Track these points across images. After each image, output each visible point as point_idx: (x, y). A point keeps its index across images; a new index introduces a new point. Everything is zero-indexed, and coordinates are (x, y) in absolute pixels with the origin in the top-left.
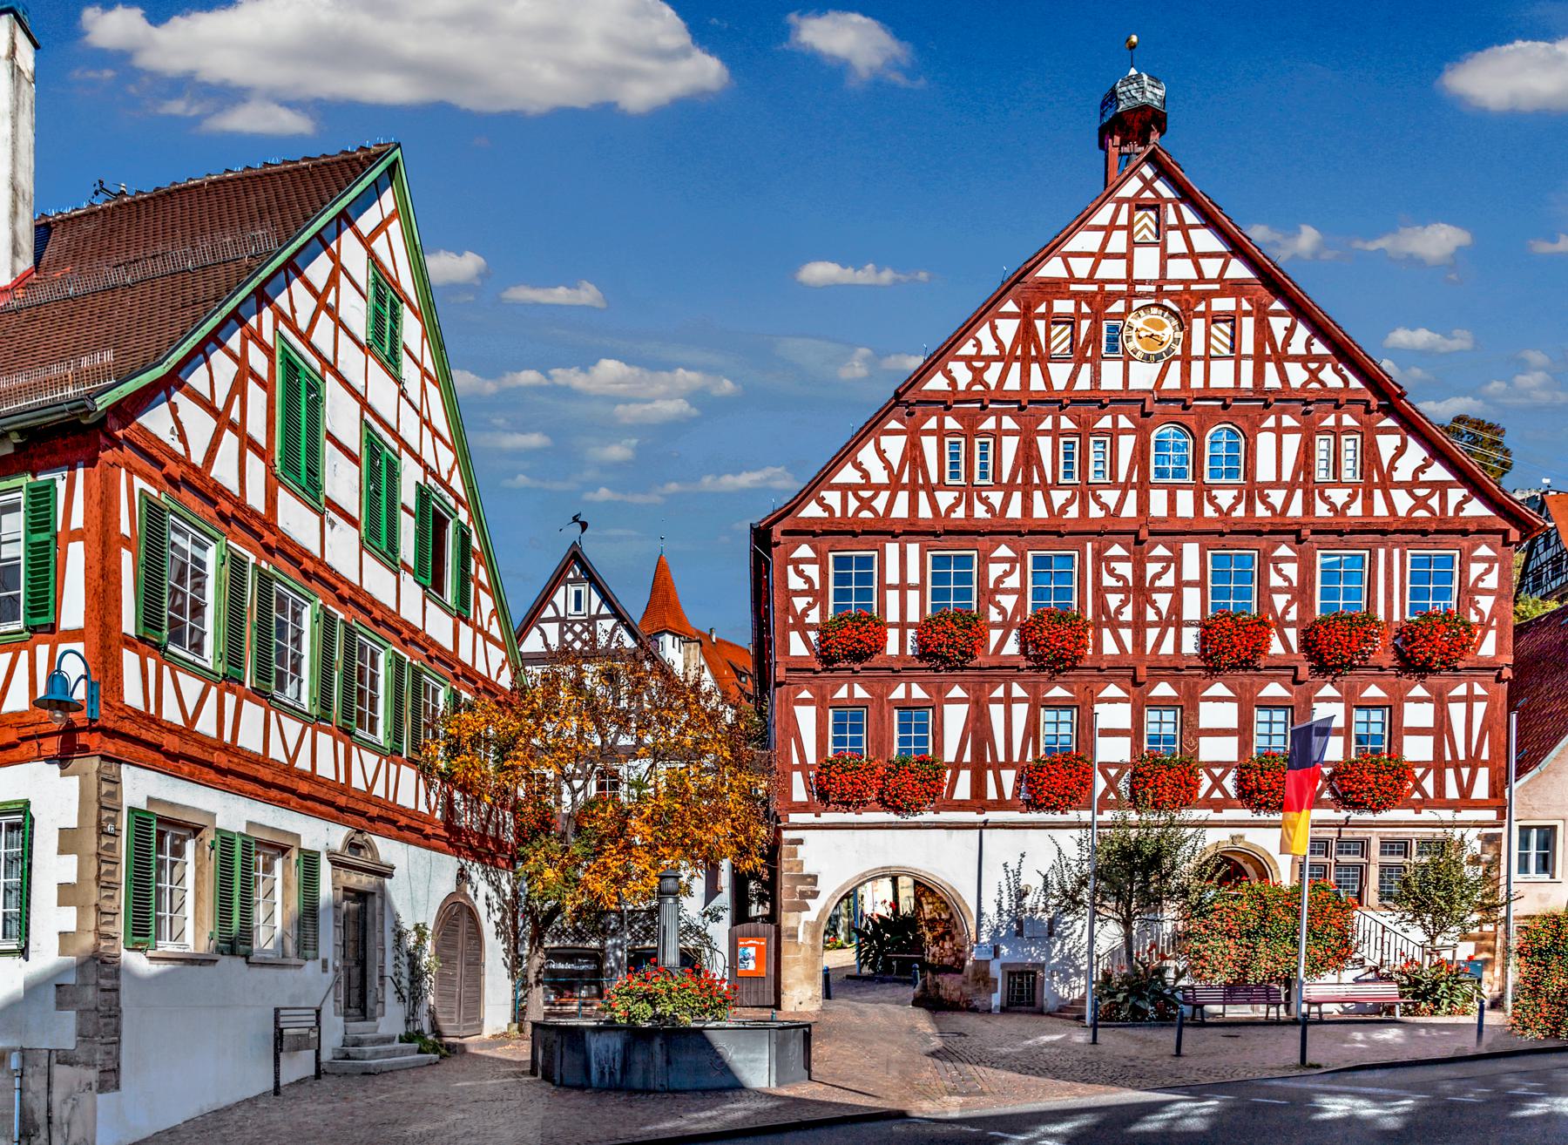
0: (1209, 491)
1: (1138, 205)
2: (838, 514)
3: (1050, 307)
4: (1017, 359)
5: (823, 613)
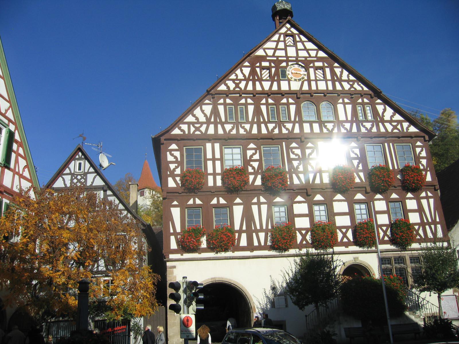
0: (324, 124)
1: (286, 35)
2: (187, 133)
3: (261, 64)
4: (251, 80)
5: (182, 170)
